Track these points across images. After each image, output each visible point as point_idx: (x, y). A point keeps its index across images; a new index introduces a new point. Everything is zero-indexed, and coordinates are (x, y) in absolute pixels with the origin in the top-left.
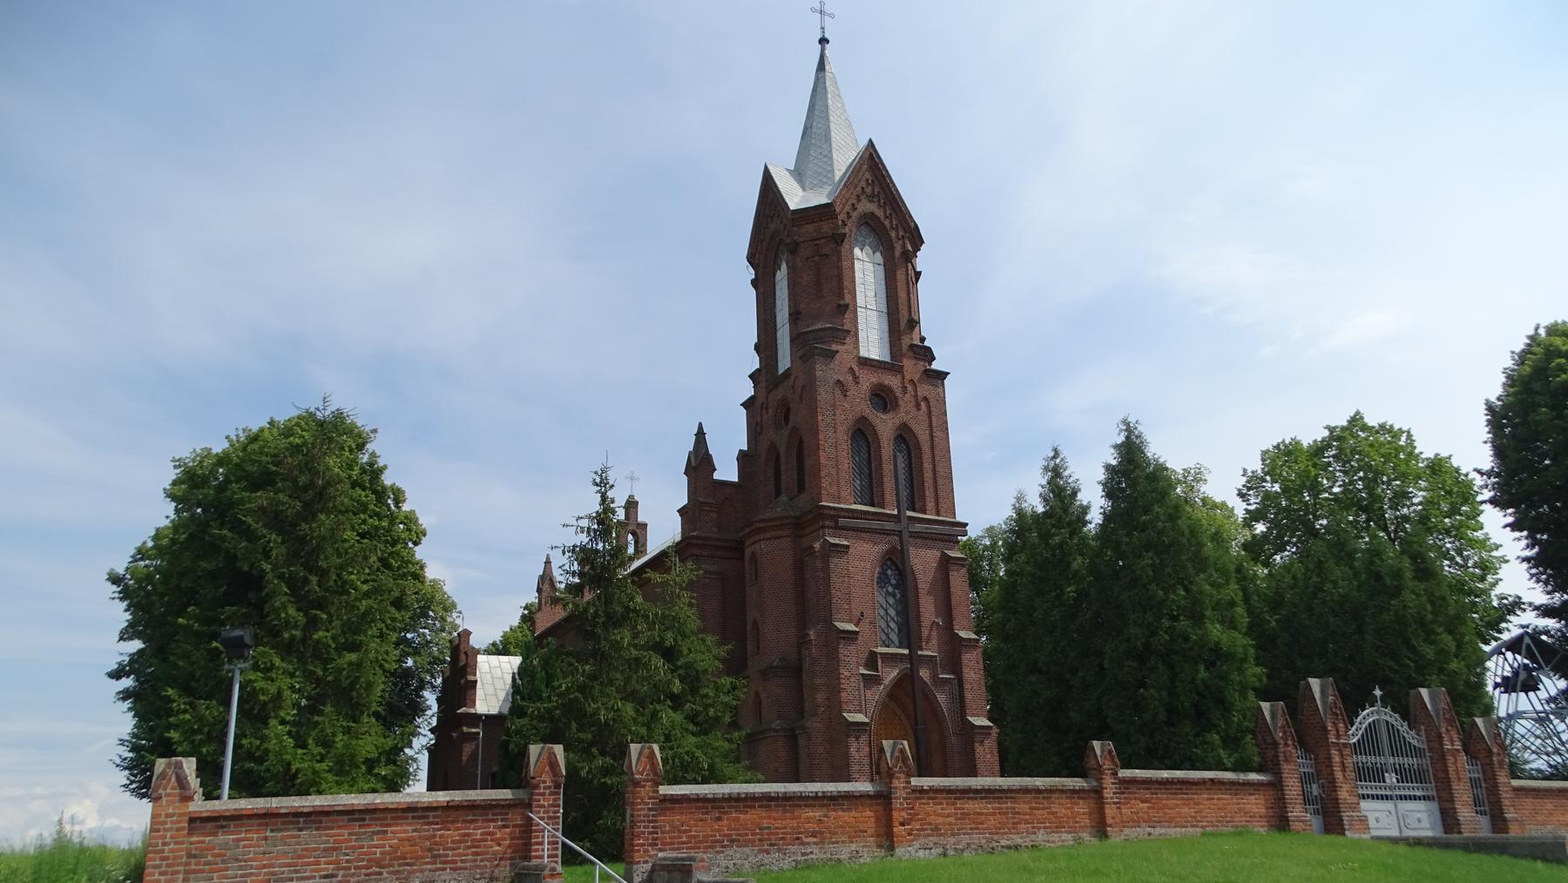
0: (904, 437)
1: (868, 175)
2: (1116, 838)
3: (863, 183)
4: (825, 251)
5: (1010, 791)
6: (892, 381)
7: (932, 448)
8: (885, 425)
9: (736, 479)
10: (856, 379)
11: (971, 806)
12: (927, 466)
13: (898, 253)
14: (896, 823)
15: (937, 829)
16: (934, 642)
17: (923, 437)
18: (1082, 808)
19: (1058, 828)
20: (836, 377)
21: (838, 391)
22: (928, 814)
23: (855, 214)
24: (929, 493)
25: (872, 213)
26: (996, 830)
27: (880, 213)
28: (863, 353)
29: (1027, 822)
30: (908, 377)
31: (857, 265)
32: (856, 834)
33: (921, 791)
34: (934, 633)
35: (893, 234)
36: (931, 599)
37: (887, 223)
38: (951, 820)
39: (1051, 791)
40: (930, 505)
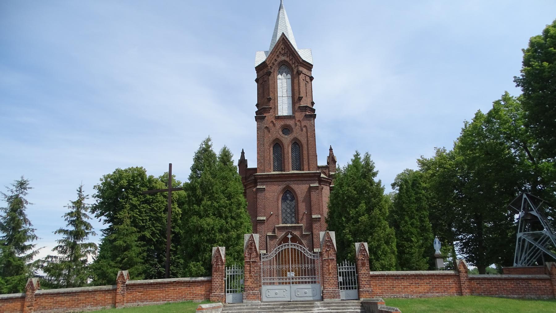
0: (296, 144)
1: (282, 46)
2: (119, 307)
3: (280, 50)
4: (265, 79)
5: (76, 292)
6: (291, 122)
7: (308, 145)
8: (287, 140)
9: (248, 167)
10: (274, 125)
11: (60, 299)
12: (305, 152)
13: (295, 73)
14: (25, 306)
15: (45, 307)
16: (305, 220)
17: (303, 141)
18: (109, 296)
19: (97, 304)
20: (265, 126)
21: (266, 131)
22: (42, 303)
23: (276, 63)
24: (305, 163)
25: (285, 60)
26: (69, 307)
27: (288, 59)
28: (280, 114)
29: (83, 303)
30: (297, 119)
31: (279, 81)
32: (446, 289)
33: (39, 295)
34: (305, 217)
35: (293, 66)
36: (304, 204)
37: (291, 62)
38: (51, 304)
39: (95, 291)
40: (306, 167)
